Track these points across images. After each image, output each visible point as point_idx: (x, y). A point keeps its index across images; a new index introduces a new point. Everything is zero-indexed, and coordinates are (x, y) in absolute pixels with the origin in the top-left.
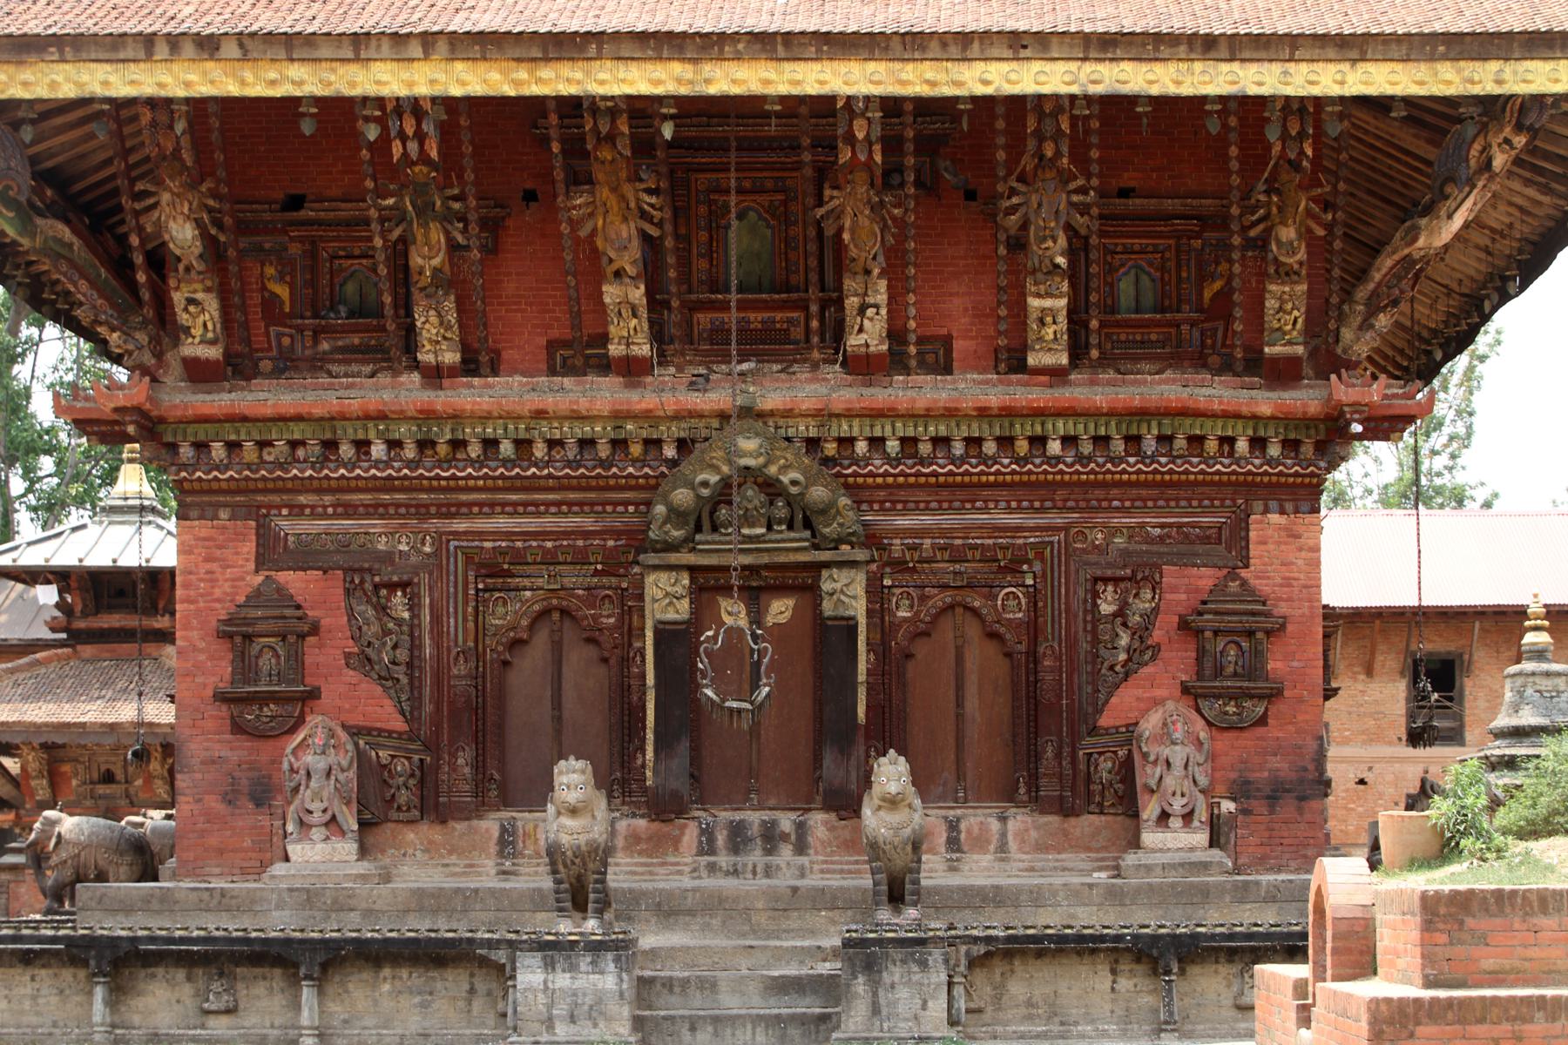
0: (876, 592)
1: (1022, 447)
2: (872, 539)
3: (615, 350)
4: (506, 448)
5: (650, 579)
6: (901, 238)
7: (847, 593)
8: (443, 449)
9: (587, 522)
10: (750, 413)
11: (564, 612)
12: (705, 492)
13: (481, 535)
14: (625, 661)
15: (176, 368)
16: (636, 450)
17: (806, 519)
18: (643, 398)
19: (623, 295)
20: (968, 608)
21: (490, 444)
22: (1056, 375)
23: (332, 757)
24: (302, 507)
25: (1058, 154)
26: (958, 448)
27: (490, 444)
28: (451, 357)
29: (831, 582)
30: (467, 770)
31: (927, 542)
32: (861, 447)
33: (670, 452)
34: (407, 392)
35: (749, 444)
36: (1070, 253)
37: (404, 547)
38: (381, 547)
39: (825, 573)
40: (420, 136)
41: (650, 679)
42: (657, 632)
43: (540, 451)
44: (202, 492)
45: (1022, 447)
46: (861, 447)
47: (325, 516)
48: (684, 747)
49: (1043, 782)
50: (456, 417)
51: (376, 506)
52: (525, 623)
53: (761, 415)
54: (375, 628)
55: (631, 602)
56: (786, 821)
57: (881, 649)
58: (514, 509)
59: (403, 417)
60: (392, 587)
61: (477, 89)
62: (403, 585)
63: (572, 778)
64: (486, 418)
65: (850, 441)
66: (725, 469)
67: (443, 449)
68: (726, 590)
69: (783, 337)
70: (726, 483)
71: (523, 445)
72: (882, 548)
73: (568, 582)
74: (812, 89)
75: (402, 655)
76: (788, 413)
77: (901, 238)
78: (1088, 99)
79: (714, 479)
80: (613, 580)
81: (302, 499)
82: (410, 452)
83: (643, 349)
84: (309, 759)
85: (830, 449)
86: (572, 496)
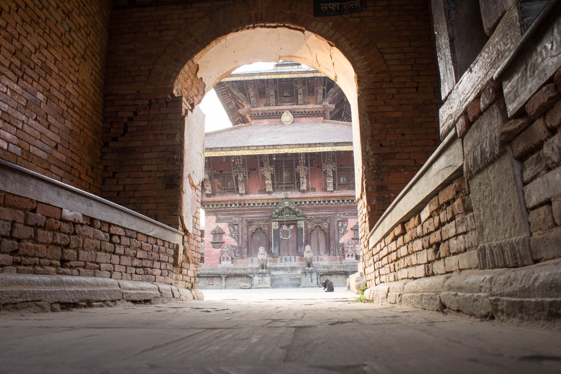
1: (327, 202)
2: (305, 216)
4: (252, 205)
7: (301, 224)
8: (243, 205)
9: (263, 215)
10: (286, 198)
11: (260, 228)
14: (269, 235)
16: (270, 204)
17: (295, 213)
19: (269, 182)
20: (319, 226)
21: (249, 204)
23: (227, 249)
26: (317, 203)
27: (249, 204)
28: (244, 192)
29: (299, 223)
32: (303, 203)
33: (275, 204)
34: (238, 197)
35: (287, 203)
36: (333, 174)
40: (240, 161)
43: (256, 205)
45: (327, 202)
46: (303, 203)
53: (288, 199)
55: (270, 227)
56: (293, 258)
57: (306, 232)
58: (253, 213)
61: (248, 154)
63: (262, 250)
64: (249, 200)
65: (301, 202)
67: (243, 205)
68: (284, 224)
69: (291, 187)
70: (283, 209)
71: (254, 204)
74: (295, 152)
76: (292, 198)
82: (238, 205)
83: (271, 190)
84: (224, 250)
85: (298, 203)
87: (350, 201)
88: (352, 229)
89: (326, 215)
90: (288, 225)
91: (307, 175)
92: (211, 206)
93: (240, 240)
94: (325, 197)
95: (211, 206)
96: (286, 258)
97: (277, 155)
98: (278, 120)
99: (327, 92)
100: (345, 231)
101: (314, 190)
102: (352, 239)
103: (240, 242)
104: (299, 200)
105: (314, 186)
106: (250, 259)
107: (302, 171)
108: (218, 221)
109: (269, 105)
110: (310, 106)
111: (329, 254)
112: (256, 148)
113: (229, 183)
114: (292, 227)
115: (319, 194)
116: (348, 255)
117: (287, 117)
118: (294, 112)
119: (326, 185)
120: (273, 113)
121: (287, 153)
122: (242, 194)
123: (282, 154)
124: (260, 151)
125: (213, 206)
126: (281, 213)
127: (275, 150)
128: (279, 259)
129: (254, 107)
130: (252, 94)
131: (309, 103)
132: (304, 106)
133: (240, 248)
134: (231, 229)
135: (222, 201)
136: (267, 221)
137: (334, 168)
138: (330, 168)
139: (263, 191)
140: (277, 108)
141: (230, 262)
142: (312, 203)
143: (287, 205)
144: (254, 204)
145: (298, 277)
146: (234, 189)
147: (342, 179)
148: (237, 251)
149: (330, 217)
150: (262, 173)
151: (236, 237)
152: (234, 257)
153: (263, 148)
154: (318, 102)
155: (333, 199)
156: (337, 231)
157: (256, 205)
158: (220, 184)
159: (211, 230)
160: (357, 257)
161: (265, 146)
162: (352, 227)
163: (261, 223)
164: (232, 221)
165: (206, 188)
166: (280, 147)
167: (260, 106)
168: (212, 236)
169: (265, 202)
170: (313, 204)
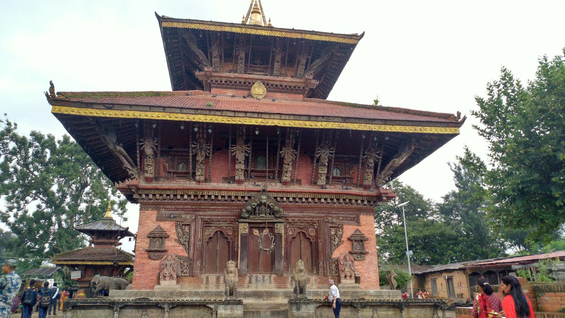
0: (286, 229)
1: (316, 200)
4: (213, 197)
5: (240, 225)
6: (296, 159)
7: (280, 228)
8: (199, 197)
11: (221, 232)
12: (254, 207)
14: (234, 242)
15: (142, 179)
16: (240, 198)
17: (273, 213)
18: (242, 187)
19: (241, 166)
21: (210, 196)
22: (322, 187)
23: (173, 262)
25: (329, 143)
26: (304, 200)
28: (202, 178)
30: (199, 265)
31: (296, 219)
32: (285, 199)
33: (246, 199)
34: (193, 185)
35: (264, 197)
36: (328, 163)
39: (276, 224)
41: (239, 246)
42: (241, 236)
43: (220, 198)
46: (285, 199)
47: (172, 210)
48: (246, 261)
49: (320, 269)
50: (203, 190)
52: (213, 233)
57: (286, 240)
58: (214, 210)
59: (191, 189)
60: (185, 225)
62: (188, 225)
65: (282, 198)
67: (199, 197)
71: (216, 196)
72: (287, 220)
73: (222, 225)
75: (188, 240)
77: (296, 159)
78: (341, 130)
79: (256, 204)
82: (192, 197)
83: (242, 178)
86: (225, 208)
87: (347, 200)
88: (349, 239)
89: (314, 217)
90: (261, 229)
91: (294, 162)
92: (151, 196)
93: (192, 248)
94: (314, 193)
95: (151, 196)
96: (257, 277)
97: (263, 128)
98: (246, 93)
99: (311, 63)
100: (341, 242)
101: (299, 182)
102: (350, 253)
103: (192, 251)
104: (280, 195)
105: (299, 178)
106: (204, 277)
107: (288, 154)
108: (160, 219)
109: (236, 72)
110: (289, 79)
111: (318, 273)
112: (232, 114)
113: (181, 165)
114: (266, 232)
115: (306, 188)
116: (346, 276)
117: (258, 90)
118: (268, 85)
119: (317, 177)
120: (240, 83)
121: (276, 127)
122: (199, 182)
123: (270, 126)
124: (238, 119)
125: (154, 195)
126: (253, 212)
127: (261, 120)
128: (247, 279)
129: (216, 72)
130: (215, 53)
131: (286, 76)
132: (280, 78)
133: (190, 261)
134: (180, 230)
135: (169, 189)
136: (231, 222)
137: (331, 154)
138: (325, 155)
139: (230, 179)
140: (246, 76)
141: (174, 282)
142: (297, 200)
143: (264, 201)
144: (216, 196)
145: (283, 308)
146: (189, 173)
147: (335, 171)
148: (186, 264)
149: (318, 221)
150: (232, 153)
151: (186, 243)
152: (180, 273)
153: (243, 115)
154: (298, 75)
155: (325, 196)
156: (328, 240)
158: (167, 165)
159: (148, 232)
160: (357, 280)
161: (246, 112)
162: (349, 236)
163: (223, 224)
164: (181, 220)
165: (146, 168)
166: (267, 116)
167: (223, 72)
168: (148, 240)
170: (299, 201)
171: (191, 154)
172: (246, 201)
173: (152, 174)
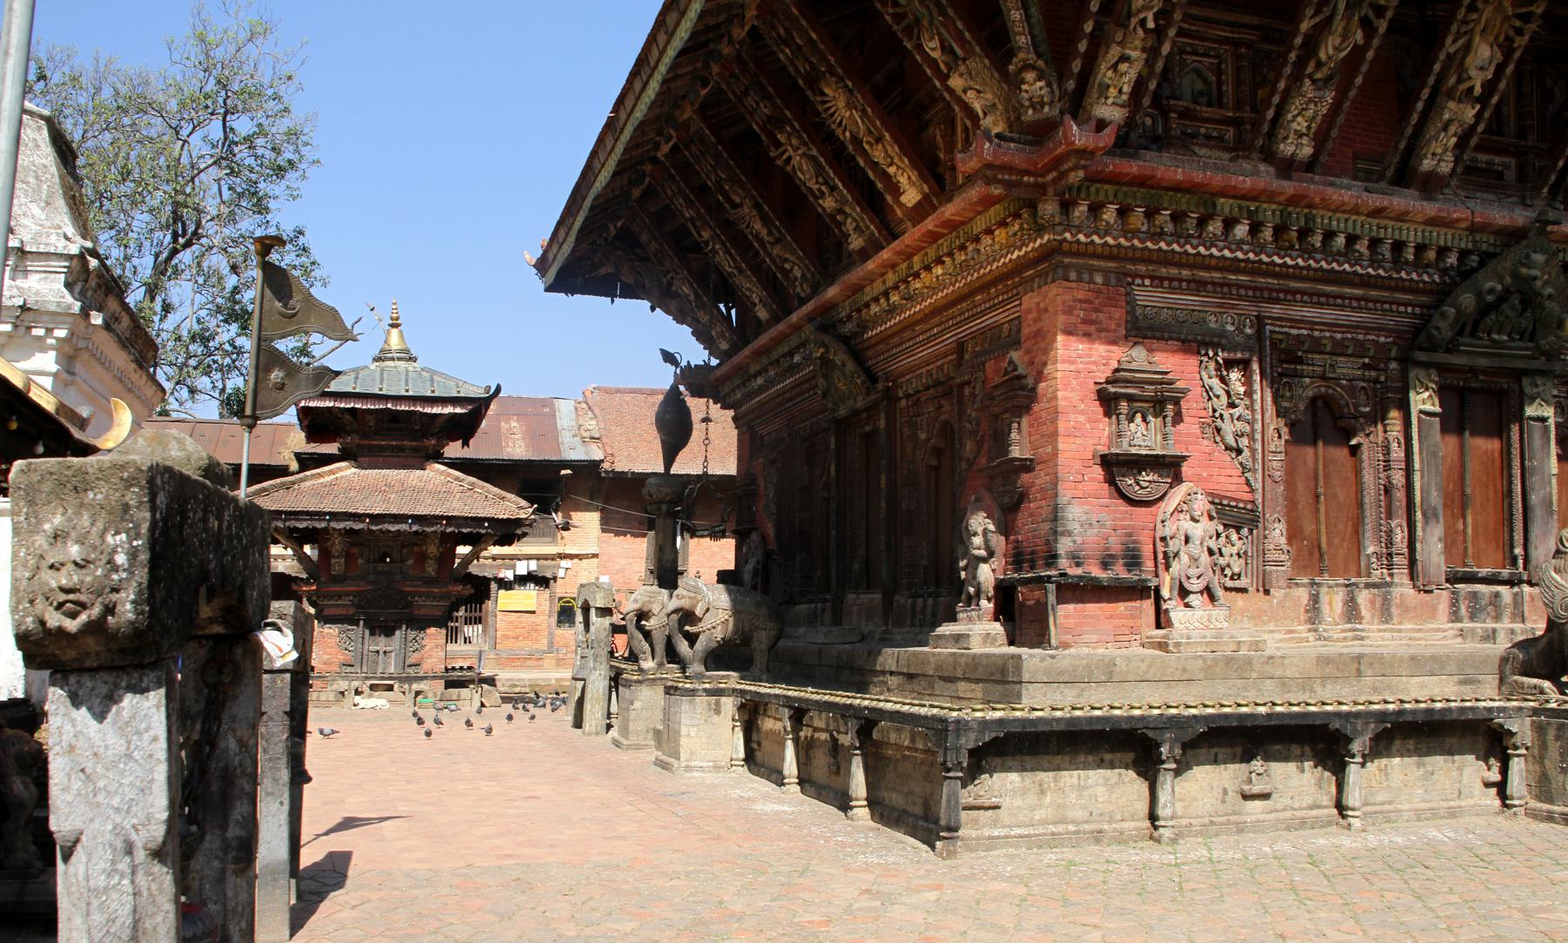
3: (1427, 164)
4: (1340, 241)
12: (1490, 298)
13: (1295, 323)
16: (1431, 255)
24: (1162, 279)
27: (1329, 235)
28: (1307, 151)
33: (1452, 260)
35: (1539, 258)
37: (1230, 328)
38: (1212, 325)
43: (1362, 247)
44: (1077, 254)
47: (1181, 291)
51: (1222, 285)
54: (1224, 399)
66: (1508, 280)
71: (1352, 239)
80: (1373, 373)
81: (1163, 271)
82: (1267, 234)
83: (1446, 168)
92: (1109, 214)
95: (1109, 214)
122: (1287, 167)
125: (1123, 213)
157: (1362, 247)
163: (1346, 368)
169: (1412, 236)
171: (1305, 26)
172: (1444, 271)
173: (1122, 106)
